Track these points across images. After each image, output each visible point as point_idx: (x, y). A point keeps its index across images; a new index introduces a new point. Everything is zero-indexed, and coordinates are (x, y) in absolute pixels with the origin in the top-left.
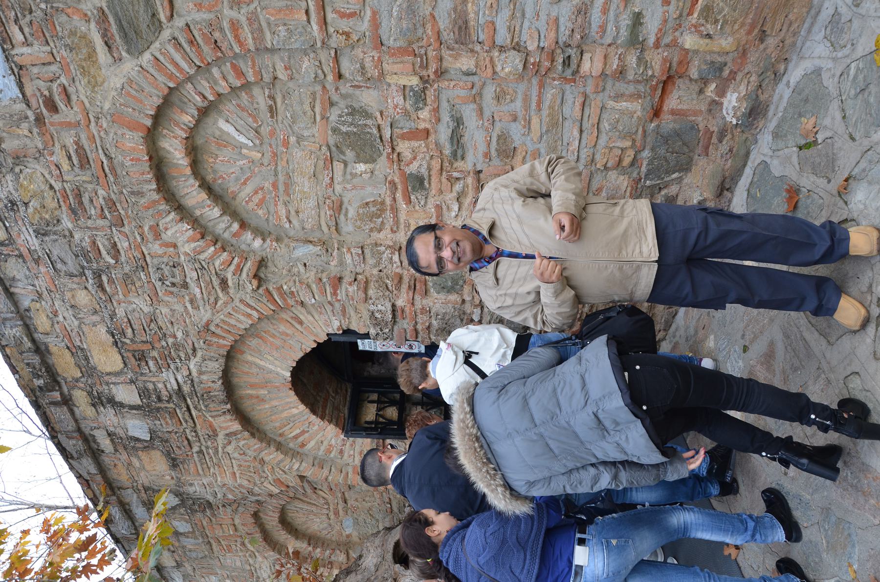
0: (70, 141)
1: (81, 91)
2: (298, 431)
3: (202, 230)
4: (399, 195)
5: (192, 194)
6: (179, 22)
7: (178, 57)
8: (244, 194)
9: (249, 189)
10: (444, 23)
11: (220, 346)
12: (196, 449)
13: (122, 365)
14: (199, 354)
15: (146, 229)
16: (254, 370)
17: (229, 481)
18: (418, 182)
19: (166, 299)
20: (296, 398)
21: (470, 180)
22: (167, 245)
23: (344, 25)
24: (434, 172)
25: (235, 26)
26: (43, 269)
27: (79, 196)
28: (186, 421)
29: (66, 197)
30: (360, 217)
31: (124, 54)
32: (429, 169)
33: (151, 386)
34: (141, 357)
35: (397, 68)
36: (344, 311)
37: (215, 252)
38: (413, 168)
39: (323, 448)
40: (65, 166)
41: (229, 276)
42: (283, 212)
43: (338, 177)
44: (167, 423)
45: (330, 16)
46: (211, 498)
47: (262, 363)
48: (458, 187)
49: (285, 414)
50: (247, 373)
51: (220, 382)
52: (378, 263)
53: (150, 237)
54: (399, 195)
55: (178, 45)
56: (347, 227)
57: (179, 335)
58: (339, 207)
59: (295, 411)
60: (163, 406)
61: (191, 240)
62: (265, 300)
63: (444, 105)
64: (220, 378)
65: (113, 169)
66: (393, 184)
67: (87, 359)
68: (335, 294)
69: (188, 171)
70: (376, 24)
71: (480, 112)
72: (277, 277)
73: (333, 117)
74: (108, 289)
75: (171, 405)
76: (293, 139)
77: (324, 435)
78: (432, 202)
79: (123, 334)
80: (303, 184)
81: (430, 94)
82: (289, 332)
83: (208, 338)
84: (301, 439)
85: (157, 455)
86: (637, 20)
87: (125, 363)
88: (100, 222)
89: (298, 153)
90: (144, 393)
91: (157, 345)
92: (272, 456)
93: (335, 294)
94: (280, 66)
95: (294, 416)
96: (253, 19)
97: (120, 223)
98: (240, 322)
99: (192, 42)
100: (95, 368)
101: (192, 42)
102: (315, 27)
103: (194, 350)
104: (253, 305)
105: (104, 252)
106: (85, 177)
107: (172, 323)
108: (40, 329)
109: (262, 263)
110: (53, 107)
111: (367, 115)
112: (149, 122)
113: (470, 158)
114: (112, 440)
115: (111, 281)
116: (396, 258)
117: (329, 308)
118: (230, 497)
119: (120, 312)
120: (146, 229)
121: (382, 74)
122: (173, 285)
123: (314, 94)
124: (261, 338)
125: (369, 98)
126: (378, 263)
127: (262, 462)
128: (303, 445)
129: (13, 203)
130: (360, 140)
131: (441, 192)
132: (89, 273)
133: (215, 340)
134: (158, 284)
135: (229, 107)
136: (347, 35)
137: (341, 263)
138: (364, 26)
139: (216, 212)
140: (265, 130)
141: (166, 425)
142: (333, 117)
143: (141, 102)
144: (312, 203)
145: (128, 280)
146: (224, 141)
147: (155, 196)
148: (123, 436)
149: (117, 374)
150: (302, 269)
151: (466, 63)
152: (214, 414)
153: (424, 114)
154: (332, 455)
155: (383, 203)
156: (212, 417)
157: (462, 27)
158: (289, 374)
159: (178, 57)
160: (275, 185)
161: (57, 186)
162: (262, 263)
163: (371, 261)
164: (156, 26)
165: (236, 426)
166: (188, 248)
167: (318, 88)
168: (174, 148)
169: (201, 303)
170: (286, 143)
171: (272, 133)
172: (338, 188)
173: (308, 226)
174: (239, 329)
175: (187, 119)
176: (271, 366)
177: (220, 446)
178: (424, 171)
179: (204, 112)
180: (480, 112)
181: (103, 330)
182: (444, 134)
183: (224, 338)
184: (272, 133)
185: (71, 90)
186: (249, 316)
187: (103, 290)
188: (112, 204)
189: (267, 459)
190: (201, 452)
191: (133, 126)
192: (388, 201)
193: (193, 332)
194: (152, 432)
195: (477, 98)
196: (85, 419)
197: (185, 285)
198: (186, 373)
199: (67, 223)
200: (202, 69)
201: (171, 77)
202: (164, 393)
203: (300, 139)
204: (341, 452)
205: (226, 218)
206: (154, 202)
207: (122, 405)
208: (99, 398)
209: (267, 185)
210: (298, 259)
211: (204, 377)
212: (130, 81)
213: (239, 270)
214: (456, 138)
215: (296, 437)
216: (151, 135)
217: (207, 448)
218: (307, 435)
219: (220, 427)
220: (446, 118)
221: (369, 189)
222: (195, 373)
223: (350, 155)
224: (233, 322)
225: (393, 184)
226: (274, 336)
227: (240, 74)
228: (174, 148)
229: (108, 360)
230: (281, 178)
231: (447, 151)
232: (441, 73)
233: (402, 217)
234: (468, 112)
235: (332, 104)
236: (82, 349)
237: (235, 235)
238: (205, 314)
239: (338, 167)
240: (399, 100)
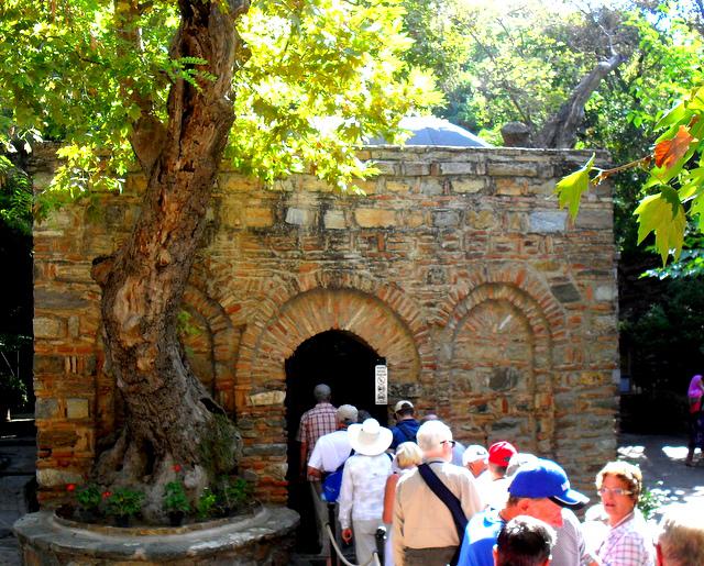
0: (510, 246)
1: (534, 260)
2: (286, 328)
3: (462, 299)
4: (474, 399)
5: (478, 298)
6: (564, 311)
7: (551, 307)
8: (473, 321)
9: (476, 324)
10: (565, 418)
11: (383, 294)
12: (277, 253)
13: (363, 225)
14: (375, 278)
15: (465, 271)
16: (352, 308)
17: (235, 269)
18: (482, 408)
19: (419, 271)
20: (323, 330)
21: (482, 433)
22: (455, 279)
23: (564, 377)
24: (486, 417)
25: (563, 334)
26: (435, 203)
27: (482, 240)
28: (311, 255)
29: (481, 233)
30: (461, 380)
31: (551, 284)
32: (489, 414)
33: (346, 240)
34: (370, 240)
35: (543, 399)
37: (452, 305)
38: (489, 405)
39: (268, 343)
40: (499, 240)
41: (437, 309)
42: (465, 339)
43: (483, 369)
45: (567, 373)
46: (211, 248)
47: (358, 314)
48: (479, 428)
49: (305, 321)
50: (348, 303)
51: (350, 286)
52: (440, 389)
53: (461, 271)
54: (474, 399)
55: (556, 308)
56: (455, 373)
57: (392, 270)
58: (467, 368)
59: (309, 328)
60: (327, 242)
61: (460, 294)
62: (421, 325)
63: (519, 420)
64: (354, 287)
65: (498, 263)
66: (481, 396)
67: (365, 204)
68: (427, 366)
69: (491, 297)
70: (565, 391)
71: (517, 436)
72: (438, 335)
73: (514, 368)
74: (424, 237)
75: (326, 249)
76: (502, 348)
77: (285, 348)
78: (471, 416)
79: (392, 236)
80: (480, 351)
81: (524, 412)
82: (387, 334)
83: (390, 288)
84: (277, 328)
85: (268, 222)
87: (364, 228)
88: (468, 247)
89: (496, 350)
90: (338, 233)
91: (382, 254)
92: (268, 308)
93: (427, 366)
94: (543, 348)
95: (303, 325)
96: (566, 341)
97: (468, 257)
98: (404, 308)
99: (557, 314)
100: (357, 206)
101: (557, 314)
102: (563, 366)
103: (380, 277)
104: (417, 319)
105: (450, 243)
106: (493, 248)
107: (401, 268)
108: (388, 183)
109: (441, 326)
110: (528, 244)
111: (515, 383)
112: (521, 286)
113: (494, 433)
114: (279, 192)
115: (430, 240)
116: (445, 398)
117: (408, 359)
118: (213, 266)
119: (407, 239)
120: (465, 271)
121: (540, 392)
122: (429, 276)
123: (523, 360)
124: (382, 316)
125: (522, 385)
126: (440, 389)
127: (261, 300)
128: (270, 329)
129: (478, 204)
130: (501, 380)
131: (476, 420)
132: (435, 229)
133: (389, 292)
134: (430, 267)
135: (518, 321)
136: (560, 379)
137: (441, 370)
138: (564, 386)
139: (469, 307)
140: (507, 336)
141: (305, 238)
142: (514, 368)
143: (531, 285)
144: (470, 356)
145: (432, 251)
146: (501, 316)
147: (484, 280)
148: (288, 203)
149: (353, 218)
150: (437, 348)
151: (544, 428)
152: (320, 277)
153: (515, 410)
154: (260, 350)
155: (470, 391)
156: (316, 275)
157: (565, 425)
158: (347, 329)
159: (551, 307)
160: (479, 337)
161: (488, 230)
162: (441, 326)
163: (441, 385)
164: (563, 301)
165: (304, 288)
166: (454, 289)
167: (527, 363)
168: (502, 293)
169: (417, 289)
170: (500, 345)
171: (505, 340)
172: (478, 369)
173: (456, 352)
174: (397, 307)
175: (518, 303)
176: (356, 320)
177: (282, 272)
178: (487, 412)
179: (518, 311)
180: (517, 436)
181: (393, 223)
182: (506, 420)
183: (390, 297)
184: (505, 340)
185: (536, 256)
186: (408, 315)
187: (426, 234)
188: (479, 256)
189: (265, 303)
190: (273, 256)
191: (520, 279)
192: (471, 394)
193: (394, 279)
194: (297, 227)
195: (524, 433)
196: (305, 180)
197: (430, 283)
198: (359, 266)
199: (466, 229)
200: (543, 315)
201: (542, 302)
202: (339, 247)
203: (502, 352)
204: (265, 357)
205: (465, 312)
206: (480, 279)
208: (326, 199)
209: (479, 334)
210: (443, 346)
211: (356, 278)
212: (540, 284)
213: (442, 316)
215: (279, 325)
216: (514, 287)
217: (278, 262)
218: (282, 333)
219: (303, 277)
220: (515, 420)
221: (478, 384)
222: (358, 272)
223: (493, 375)
224: (404, 304)
225: (481, 396)
227: (541, 330)
228: (502, 293)
229: (366, 217)
230: (483, 341)
231: (498, 422)
232: (537, 418)
233: (463, 401)
234: (518, 430)
235: (519, 368)
236: (373, 203)
237: (456, 316)
238: (409, 290)
239: (489, 370)
240: (522, 399)
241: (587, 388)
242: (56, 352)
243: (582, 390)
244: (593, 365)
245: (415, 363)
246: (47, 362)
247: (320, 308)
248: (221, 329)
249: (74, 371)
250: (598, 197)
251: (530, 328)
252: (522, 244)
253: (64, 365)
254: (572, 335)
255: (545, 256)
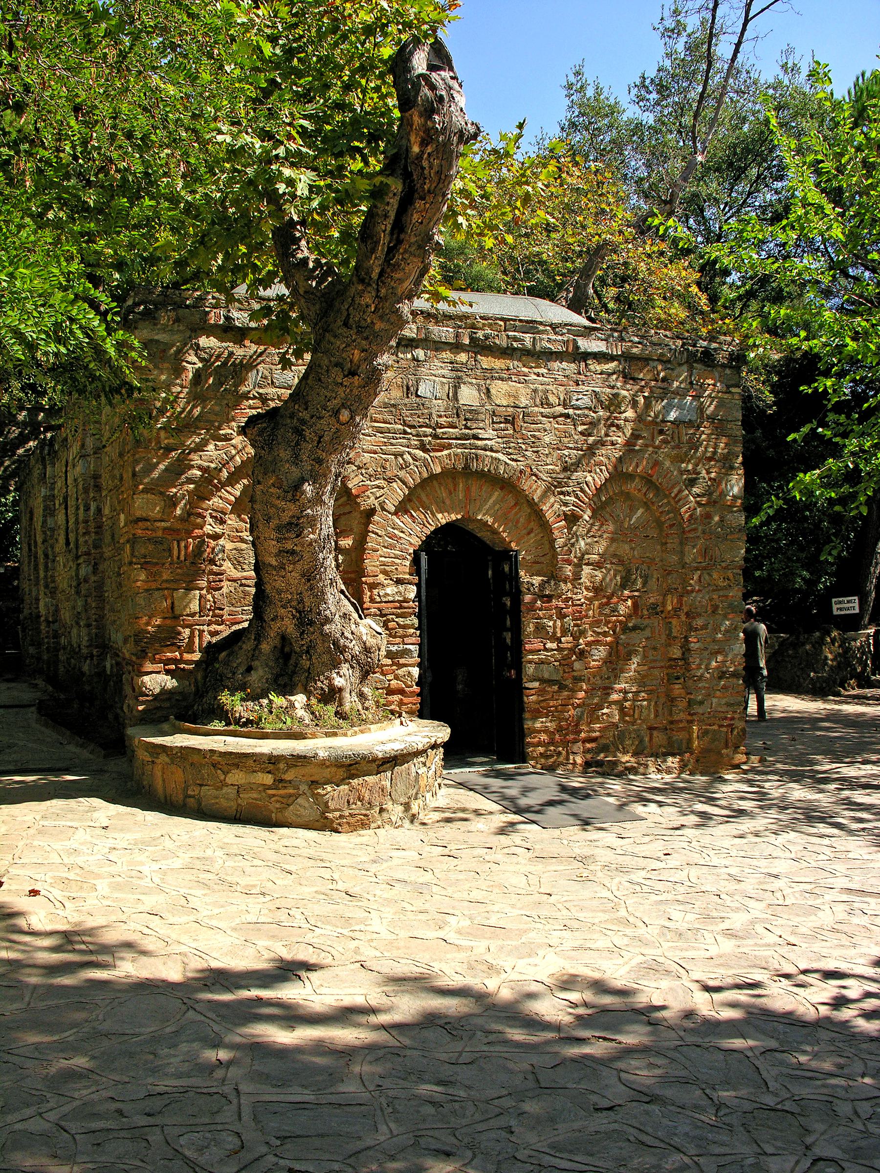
36: (538, 563)
44: (440, 416)
47: (491, 501)
86: (701, 703)
89: (627, 547)
146: (632, 510)
170: (631, 541)
189: (394, 485)
207: (456, 388)
214: (635, 628)
226: (516, 514)
234: (647, 633)
240: (652, 600)
241: (717, 589)
242: (160, 533)
243: (714, 591)
244: (723, 564)
245: (548, 557)
246: (151, 547)
247: (451, 493)
248: (344, 514)
249: (182, 558)
250: (728, 387)
251: (659, 524)
252: (656, 432)
253: (170, 550)
254: (704, 532)
255: (678, 447)
